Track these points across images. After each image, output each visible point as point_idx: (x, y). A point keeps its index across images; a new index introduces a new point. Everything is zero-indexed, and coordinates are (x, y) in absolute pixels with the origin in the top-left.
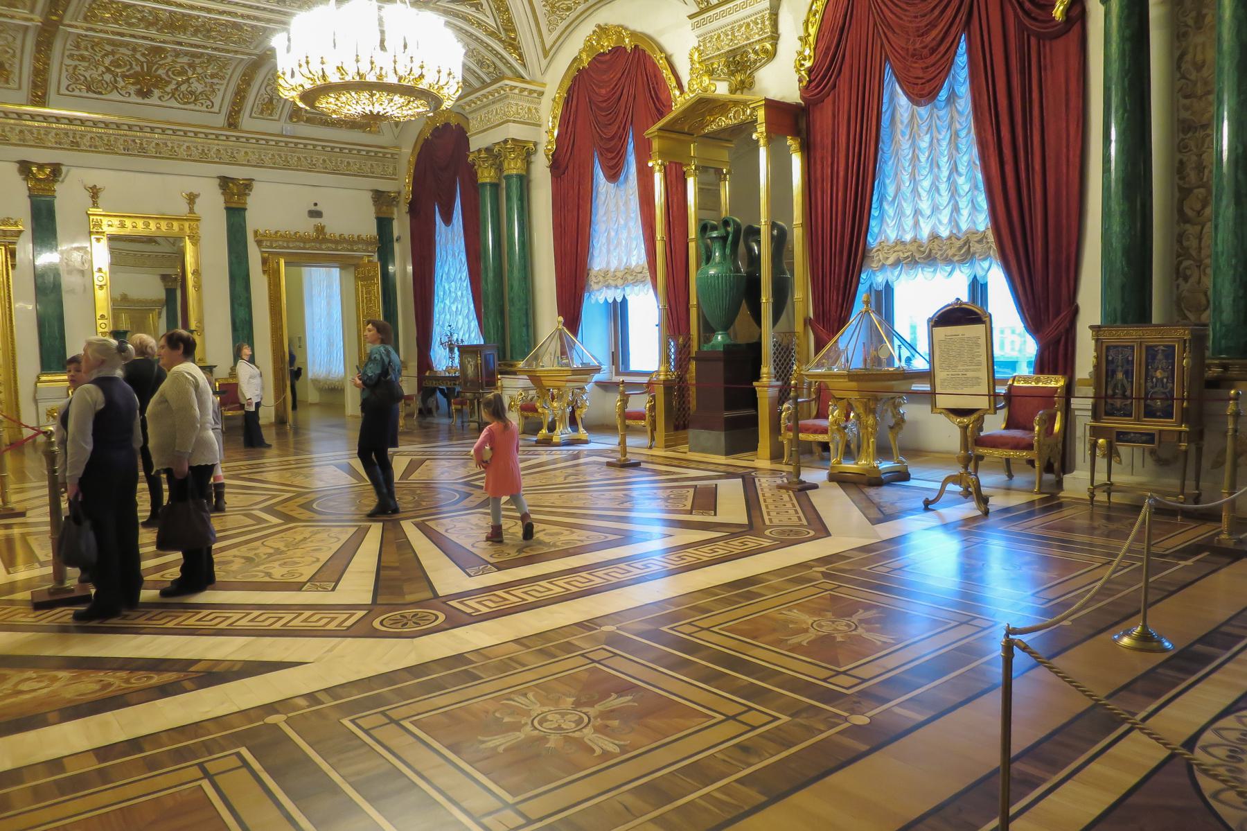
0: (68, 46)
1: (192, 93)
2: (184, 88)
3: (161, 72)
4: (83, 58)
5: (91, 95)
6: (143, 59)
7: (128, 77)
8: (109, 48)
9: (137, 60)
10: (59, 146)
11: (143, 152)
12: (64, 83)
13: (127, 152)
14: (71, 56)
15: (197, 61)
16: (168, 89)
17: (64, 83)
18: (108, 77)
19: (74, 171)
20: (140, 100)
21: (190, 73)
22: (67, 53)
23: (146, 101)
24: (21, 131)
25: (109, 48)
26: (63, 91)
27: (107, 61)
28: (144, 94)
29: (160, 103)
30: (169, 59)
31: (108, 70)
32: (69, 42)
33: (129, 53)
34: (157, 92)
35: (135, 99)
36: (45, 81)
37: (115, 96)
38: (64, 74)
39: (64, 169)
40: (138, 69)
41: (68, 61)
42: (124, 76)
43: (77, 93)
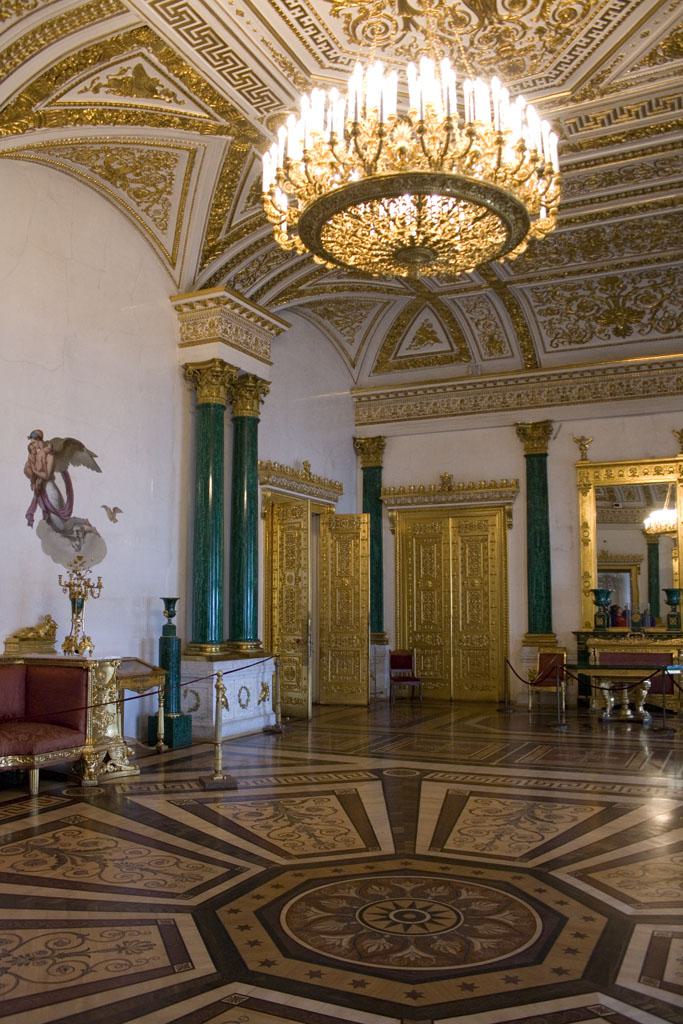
0: (533, 304)
1: (672, 318)
2: (660, 314)
3: (628, 304)
4: (553, 312)
5: (574, 346)
6: (605, 296)
7: (599, 318)
8: (567, 294)
9: (599, 299)
10: (550, 403)
11: (630, 394)
12: (547, 340)
13: (614, 396)
14: (540, 312)
15: (658, 280)
16: (645, 320)
17: (547, 340)
18: (582, 324)
19: (565, 425)
20: (621, 340)
21: (659, 296)
22: (536, 310)
23: (628, 339)
24: (519, 396)
25: (567, 294)
26: (549, 349)
27: (574, 308)
28: (624, 332)
29: (641, 338)
30: (630, 288)
31: (580, 318)
32: (531, 300)
33: (588, 293)
34: (635, 328)
35: (615, 339)
36: (530, 342)
37: (595, 342)
38: (544, 332)
39: (555, 426)
40: (607, 307)
41: (541, 319)
42: (597, 319)
43: (561, 347)
